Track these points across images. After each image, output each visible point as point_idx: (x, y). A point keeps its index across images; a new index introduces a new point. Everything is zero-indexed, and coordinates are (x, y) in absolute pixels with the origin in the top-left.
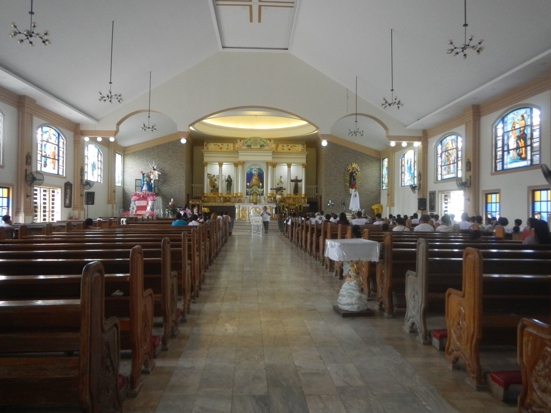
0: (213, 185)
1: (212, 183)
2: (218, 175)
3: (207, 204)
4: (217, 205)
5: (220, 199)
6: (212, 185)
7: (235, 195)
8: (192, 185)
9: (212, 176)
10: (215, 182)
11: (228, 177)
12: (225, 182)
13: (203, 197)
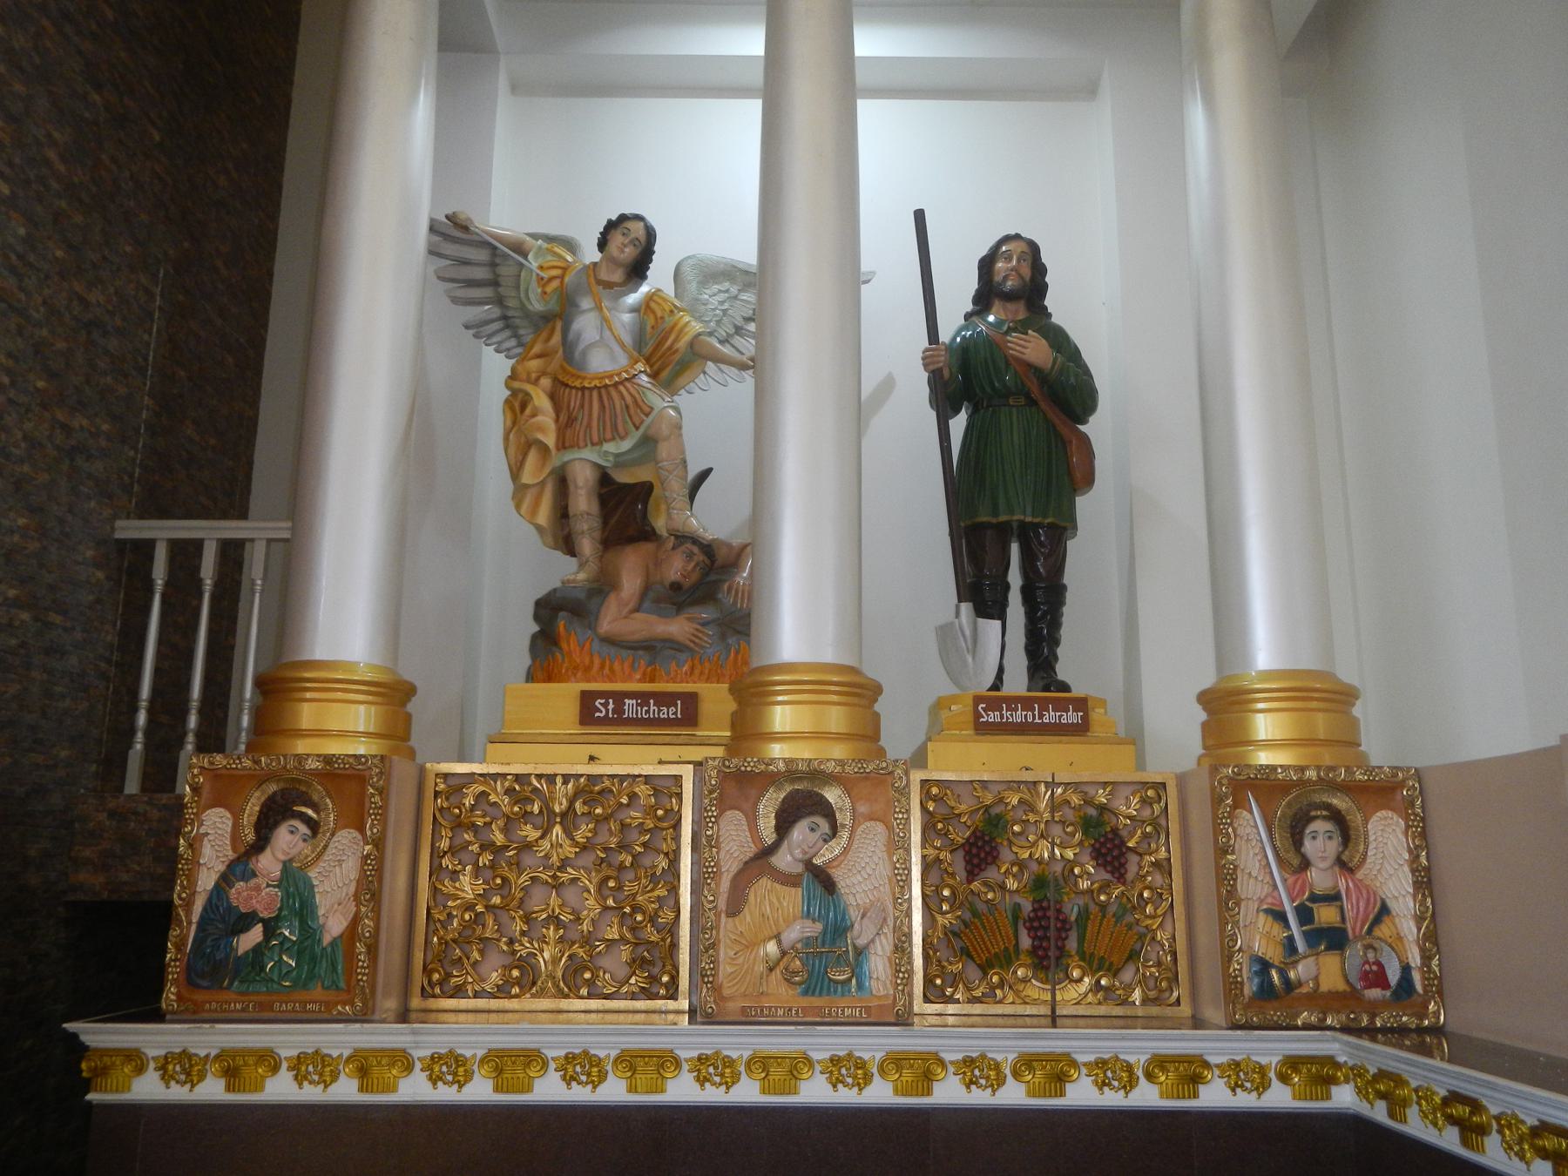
0: (583, 465)
1: (566, 423)
2: (746, 252)
3: (339, 1039)
4: (682, 1090)
5: (822, 880)
6: (562, 482)
7: (1265, 724)
8: (130, 529)
9: (592, 254)
10: (657, 400)
11: (987, 295)
12: (915, 386)
13: (225, 791)
